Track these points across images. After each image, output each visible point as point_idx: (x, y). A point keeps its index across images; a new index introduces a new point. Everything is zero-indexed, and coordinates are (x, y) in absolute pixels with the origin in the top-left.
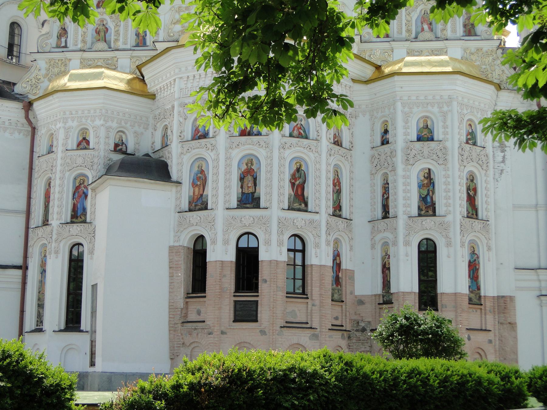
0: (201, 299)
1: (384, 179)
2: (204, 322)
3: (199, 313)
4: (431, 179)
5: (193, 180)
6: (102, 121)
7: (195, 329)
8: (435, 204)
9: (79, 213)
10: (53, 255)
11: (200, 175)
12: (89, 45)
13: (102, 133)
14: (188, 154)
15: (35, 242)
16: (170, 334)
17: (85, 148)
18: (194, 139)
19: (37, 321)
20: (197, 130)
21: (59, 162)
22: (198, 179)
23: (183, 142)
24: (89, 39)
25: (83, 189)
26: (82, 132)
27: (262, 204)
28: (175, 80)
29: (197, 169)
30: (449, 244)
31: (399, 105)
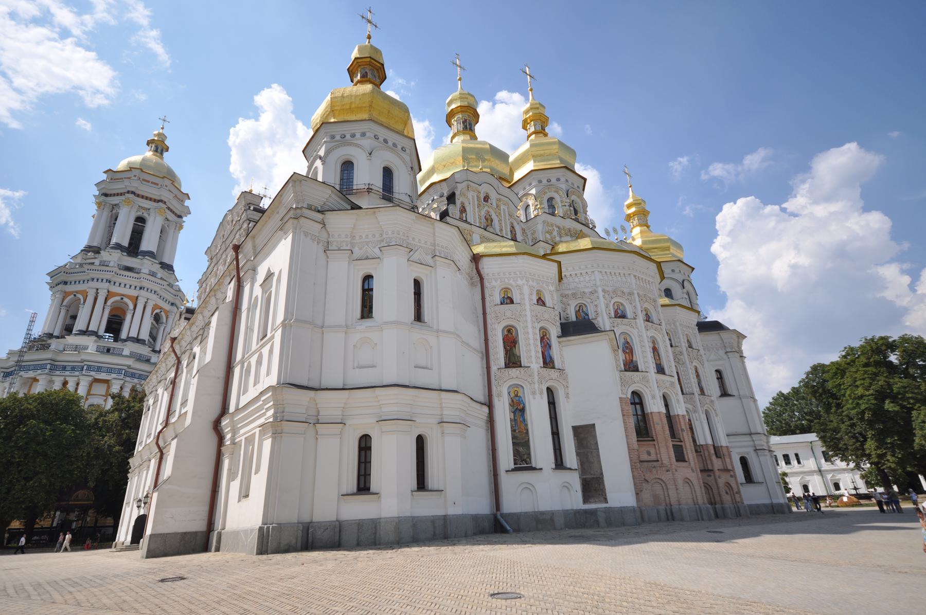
0: (651, 443)
3: (649, 454)
7: (654, 467)
9: (548, 361)
10: (538, 396)
11: (627, 345)
16: (633, 472)
18: (616, 317)
19: (515, 460)
20: (616, 312)
21: (528, 313)
22: (627, 348)
31: (678, 324)
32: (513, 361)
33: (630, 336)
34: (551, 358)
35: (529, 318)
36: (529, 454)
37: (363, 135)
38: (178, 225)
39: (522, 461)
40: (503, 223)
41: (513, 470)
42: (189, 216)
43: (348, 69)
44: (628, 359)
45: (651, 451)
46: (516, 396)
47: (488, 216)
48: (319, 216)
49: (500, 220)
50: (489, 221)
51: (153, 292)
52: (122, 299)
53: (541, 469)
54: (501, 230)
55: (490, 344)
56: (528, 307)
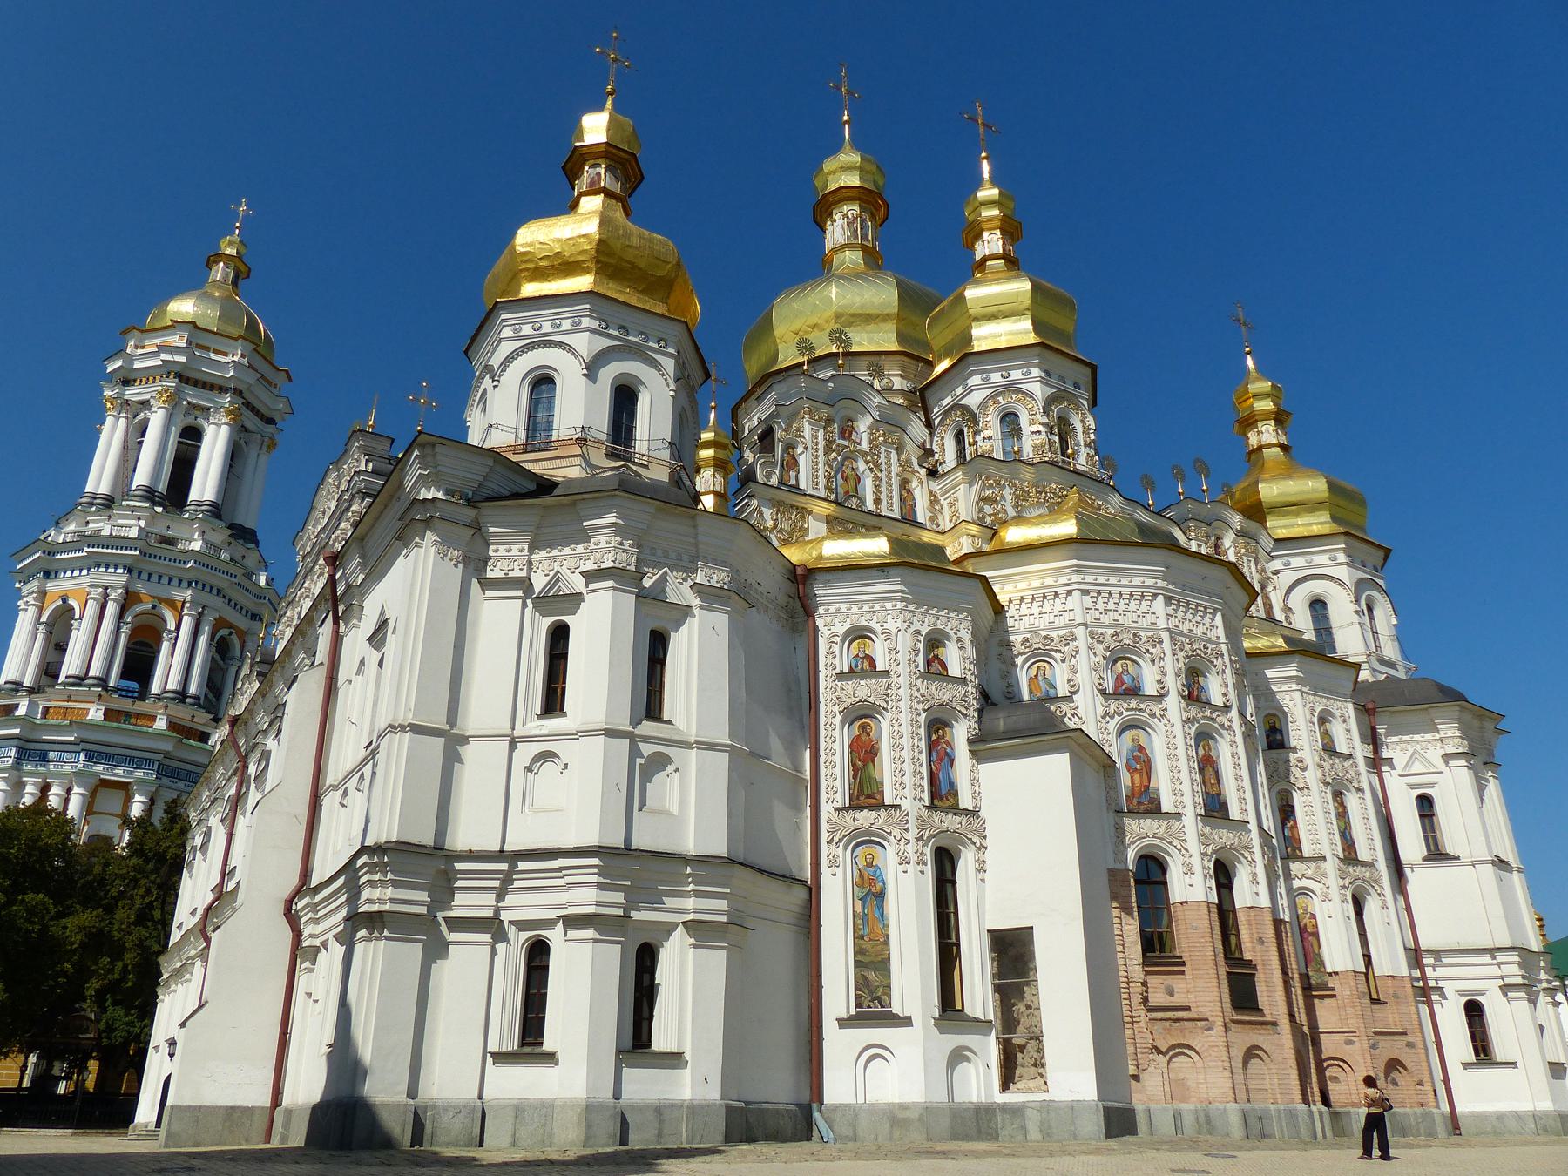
1: (1282, 799)
2: (1187, 1009)
3: (1170, 992)
4: (1345, 807)
5: (1128, 759)
6: (970, 632)
8: (1354, 843)
9: (944, 791)
13: (970, 652)
14: (1117, 718)
15: (845, 836)
20: (1119, 680)
22: (1136, 759)
23: (1103, 692)
25: (945, 746)
26: (930, 644)
27: (1235, 813)
28: (1070, 593)
29: (1131, 743)
30: (1385, 907)
33: (1147, 731)
34: (952, 785)
35: (904, 705)
36: (889, 987)
38: (266, 439)
39: (872, 1001)
40: (883, 483)
41: (851, 1018)
43: (563, 167)
44: (1137, 783)
45: (1174, 986)
46: (870, 865)
48: (471, 513)
49: (877, 478)
50: (852, 483)
51: (214, 591)
52: (154, 607)
53: (910, 1018)
54: (877, 501)
56: (903, 681)
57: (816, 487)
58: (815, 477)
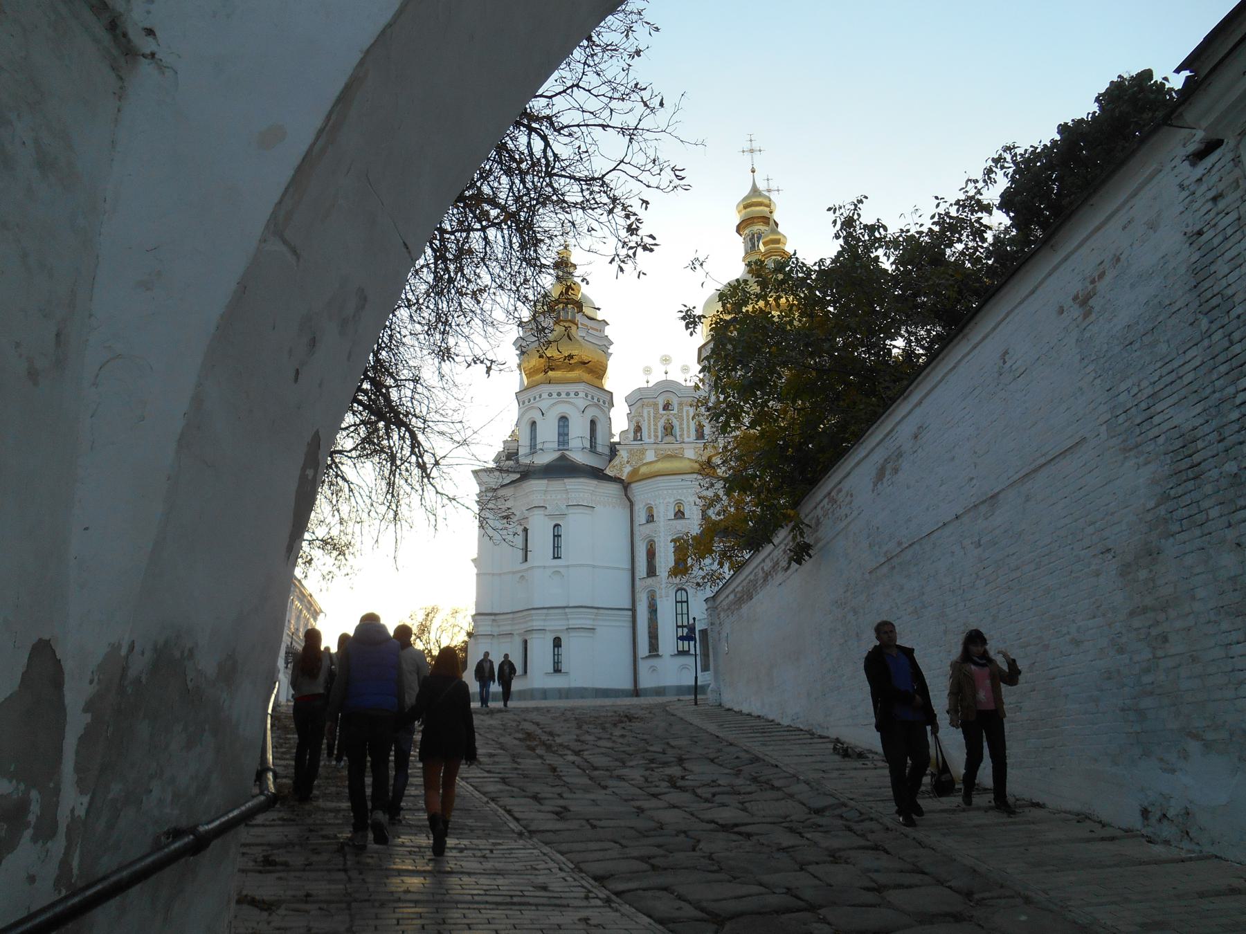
12: (660, 439)
17: (681, 518)
24: (660, 434)
32: (652, 571)
36: (658, 644)
37: (540, 396)
40: (685, 426)
41: (646, 657)
42: (611, 347)
46: (653, 599)
47: (667, 425)
50: (669, 430)
54: (681, 436)
55: (637, 559)
57: (650, 438)
58: (649, 433)
